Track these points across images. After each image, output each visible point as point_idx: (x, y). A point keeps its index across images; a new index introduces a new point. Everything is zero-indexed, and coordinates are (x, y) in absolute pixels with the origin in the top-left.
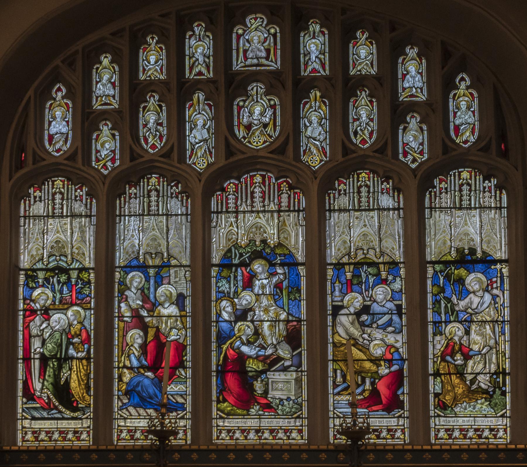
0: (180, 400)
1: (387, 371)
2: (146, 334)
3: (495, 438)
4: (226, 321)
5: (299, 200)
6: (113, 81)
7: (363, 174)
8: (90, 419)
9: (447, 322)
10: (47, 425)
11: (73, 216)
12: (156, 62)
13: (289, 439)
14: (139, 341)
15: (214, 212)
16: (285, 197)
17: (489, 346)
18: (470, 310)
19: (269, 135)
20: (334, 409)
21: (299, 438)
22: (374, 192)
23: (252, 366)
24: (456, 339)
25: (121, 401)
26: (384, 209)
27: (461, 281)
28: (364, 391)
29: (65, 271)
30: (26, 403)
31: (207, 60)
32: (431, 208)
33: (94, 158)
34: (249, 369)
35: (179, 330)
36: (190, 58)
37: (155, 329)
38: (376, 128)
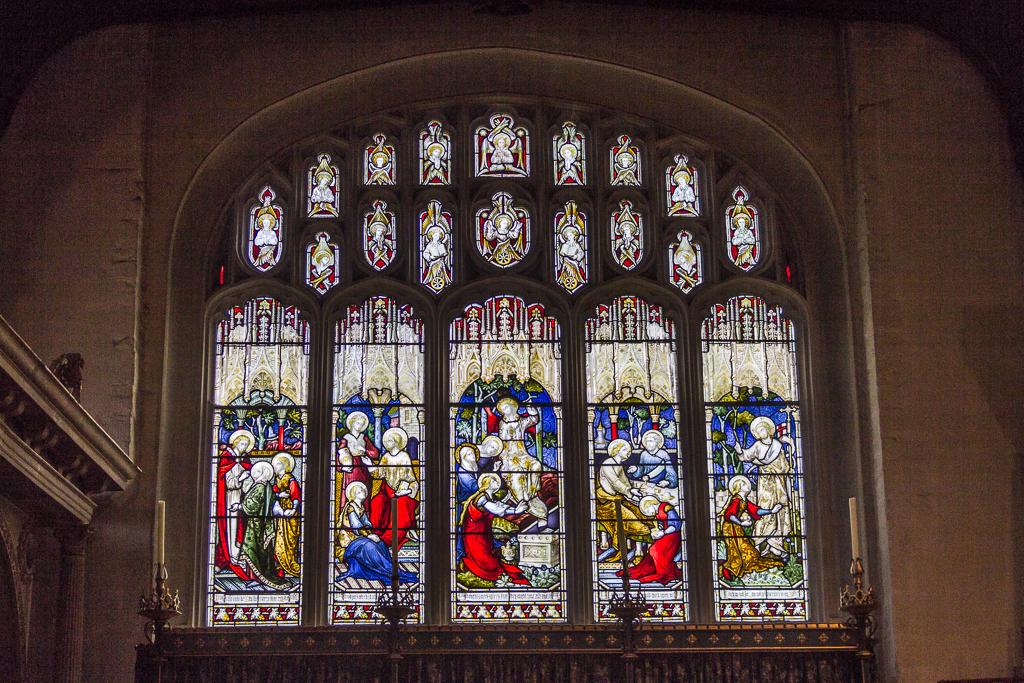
0: (412, 569)
1: (661, 533)
2: (370, 488)
3: (792, 615)
4: (467, 472)
5: (553, 328)
6: (332, 185)
7: (629, 300)
8: (300, 592)
9: (731, 475)
10: (246, 600)
11: (282, 343)
12: (384, 166)
13: (545, 617)
14: (362, 496)
15: (453, 342)
16: (536, 325)
17: (780, 503)
18: (756, 461)
19: (517, 252)
20: (599, 579)
21: (557, 615)
22: (641, 321)
23: (499, 526)
24: (742, 494)
25: (338, 569)
26: (653, 341)
27: (744, 427)
28: (634, 557)
29: (271, 410)
30: (218, 573)
31: (444, 165)
32: (708, 340)
33: (308, 276)
34: (496, 531)
35: (410, 483)
36: (424, 161)
37: (381, 482)
38: (641, 247)
